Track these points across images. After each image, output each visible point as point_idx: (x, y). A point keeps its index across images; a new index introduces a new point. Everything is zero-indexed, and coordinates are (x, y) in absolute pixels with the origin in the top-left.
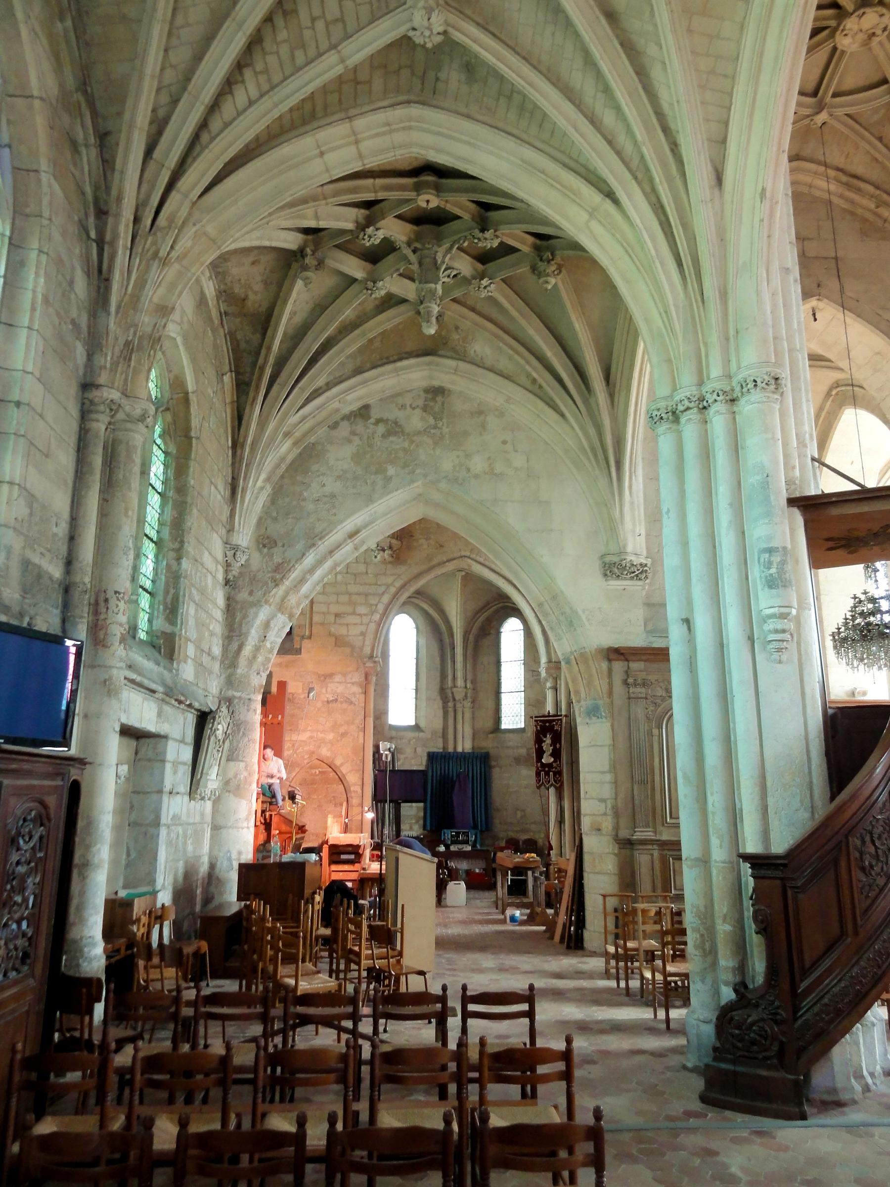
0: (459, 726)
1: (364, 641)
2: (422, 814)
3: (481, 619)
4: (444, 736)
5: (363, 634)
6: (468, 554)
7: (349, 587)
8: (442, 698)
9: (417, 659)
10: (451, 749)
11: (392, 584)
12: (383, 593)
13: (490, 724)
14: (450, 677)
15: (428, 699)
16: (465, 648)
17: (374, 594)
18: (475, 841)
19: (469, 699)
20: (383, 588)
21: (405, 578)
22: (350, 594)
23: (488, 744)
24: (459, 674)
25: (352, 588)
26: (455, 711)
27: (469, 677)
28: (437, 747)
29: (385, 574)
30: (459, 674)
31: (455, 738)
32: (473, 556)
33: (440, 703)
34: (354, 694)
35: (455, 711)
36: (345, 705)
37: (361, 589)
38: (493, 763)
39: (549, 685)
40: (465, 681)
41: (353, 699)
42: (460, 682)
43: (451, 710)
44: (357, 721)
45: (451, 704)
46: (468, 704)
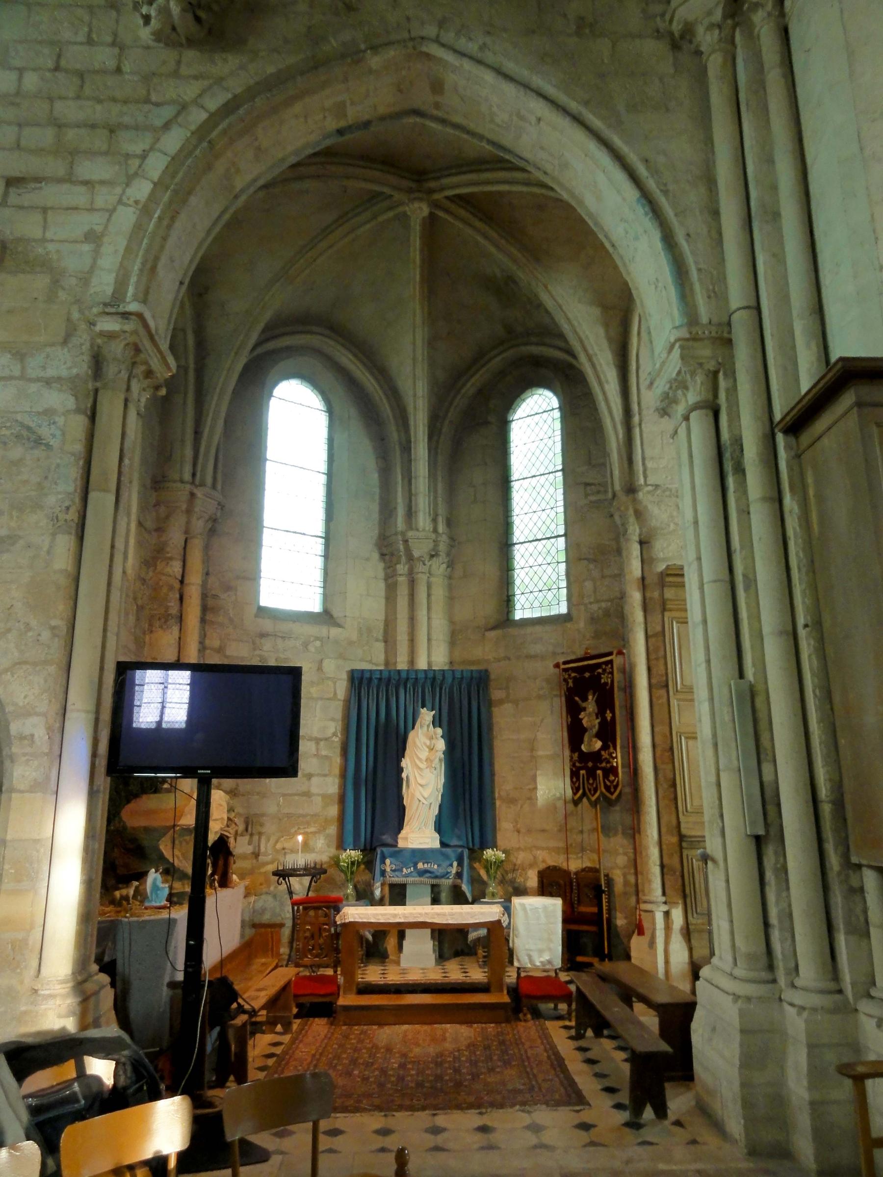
0: (422, 614)
1: (96, 254)
2: (333, 811)
3: (471, 386)
4: (388, 639)
5: (93, 238)
6: (431, 31)
7: (59, 105)
9: (330, 474)
10: (402, 665)
11: (197, 102)
12: (167, 126)
13: (489, 609)
14: (401, 512)
16: (433, 450)
17: (137, 128)
18: (459, 875)
20: (168, 112)
21: (237, 85)
22: (59, 125)
23: (484, 652)
25: (69, 110)
26: (412, 583)
28: (372, 659)
29: (176, 74)
32: (449, 37)
33: (381, 565)
34: (49, 412)
35: (412, 583)
36: (17, 452)
37: (98, 112)
38: (496, 694)
39: (692, 397)
40: (434, 521)
41: (45, 431)
43: (402, 580)
44: (51, 500)
45: (402, 568)
46: (439, 567)
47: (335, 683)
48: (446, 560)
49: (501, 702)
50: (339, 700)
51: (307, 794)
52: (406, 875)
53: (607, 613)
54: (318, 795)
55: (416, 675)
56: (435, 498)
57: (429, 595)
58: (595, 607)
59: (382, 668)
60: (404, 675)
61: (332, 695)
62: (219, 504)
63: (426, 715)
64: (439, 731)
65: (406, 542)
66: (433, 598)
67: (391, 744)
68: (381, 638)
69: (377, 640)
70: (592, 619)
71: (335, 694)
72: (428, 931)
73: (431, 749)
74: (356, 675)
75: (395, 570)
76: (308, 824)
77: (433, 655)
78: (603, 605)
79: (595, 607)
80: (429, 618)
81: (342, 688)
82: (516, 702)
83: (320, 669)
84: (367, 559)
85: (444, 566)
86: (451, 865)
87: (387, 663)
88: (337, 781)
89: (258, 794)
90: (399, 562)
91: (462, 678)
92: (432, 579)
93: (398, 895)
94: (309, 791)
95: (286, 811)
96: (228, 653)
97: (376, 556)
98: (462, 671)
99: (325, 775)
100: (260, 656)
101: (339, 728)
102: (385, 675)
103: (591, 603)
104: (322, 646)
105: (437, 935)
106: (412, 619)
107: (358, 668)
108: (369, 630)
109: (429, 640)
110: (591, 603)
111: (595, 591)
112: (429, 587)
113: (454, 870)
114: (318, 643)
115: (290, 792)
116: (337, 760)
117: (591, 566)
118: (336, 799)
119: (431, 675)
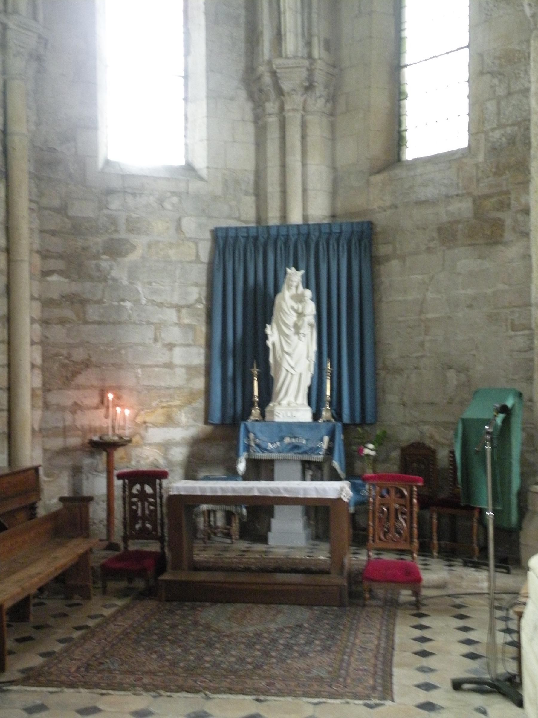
0: (295, 160)
2: (199, 383)
8: (251, 96)
15: (213, 96)
18: (330, 451)
19: (320, 90)
24: (291, 22)
27: (320, 29)
30: (291, 22)
31: (284, 192)
33: (249, 106)
38: (383, 250)
40: (309, 44)
42: (292, 44)
43: (273, 120)
45: (271, 107)
47: (196, 244)
48: (325, 93)
49: (387, 258)
50: (204, 263)
51: (169, 366)
52: (272, 449)
53: (512, 141)
54: (181, 366)
55: (288, 231)
56: (310, 14)
57: (304, 137)
58: (497, 134)
59: (253, 225)
60: (273, 232)
61: (194, 258)
62: (40, 37)
63: (295, 276)
64: (308, 293)
65: (274, 73)
66: (309, 139)
67: (260, 308)
68: (251, 191)
69: (246, 193)
70: (494, 149)
71: (198, 256)
72: (299, 510)
73: (301, 315)
74: (220, 234)
75: (264, 110)
76: (171, 397)
77: (310, 204)
78: (509, 130)
79: (497, 134)
80: (304, 165)
81: (205, 250)
82: (403, 258)
83: (179, 228)
84: (232, 99)
85: (323, 100)
86: (322, 440)
87: (259, 220)
88: (202, 351)
89: (114, 365)
90: (268, 100)
91: (341, 233)
92: (309, 118)
93: (260, 469)
94: (171, 362)
95: (146, 383)
96: (71, 213)
97: (243, 94)
98: (341, 225)
99: (189, 345)
100: (108, 216)
101: (204, 293)
102: (253, 233)
103: (493, 130)
104: (180, 202)
105: (312, 514)
106: (283, 166)
107: (224, 225)
108: (237, 182)
109: (305, 191)
110: (493, 130)
111: (499, 114)
112: (304, 126)
113: (325, 445)
114: (175, 200)
115: (149, 363)
116: (202, 329)
117: (496, 81)
118: (202, 371)
119: (304, 231)
